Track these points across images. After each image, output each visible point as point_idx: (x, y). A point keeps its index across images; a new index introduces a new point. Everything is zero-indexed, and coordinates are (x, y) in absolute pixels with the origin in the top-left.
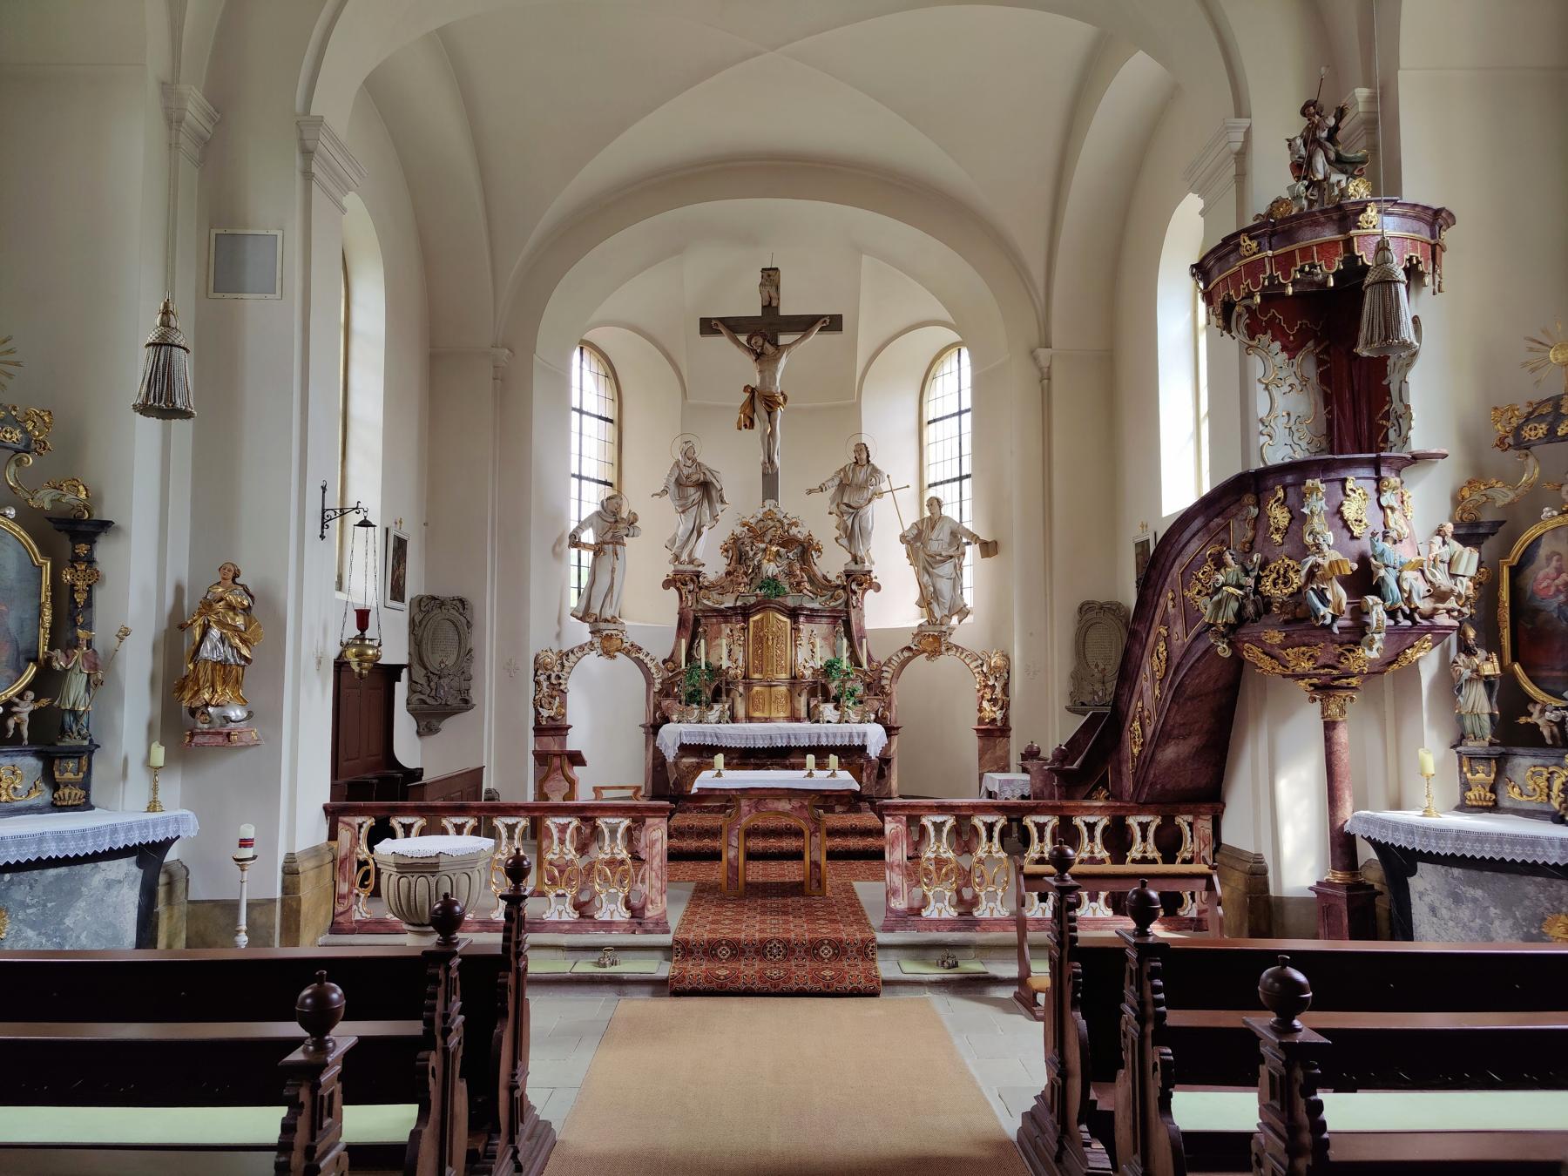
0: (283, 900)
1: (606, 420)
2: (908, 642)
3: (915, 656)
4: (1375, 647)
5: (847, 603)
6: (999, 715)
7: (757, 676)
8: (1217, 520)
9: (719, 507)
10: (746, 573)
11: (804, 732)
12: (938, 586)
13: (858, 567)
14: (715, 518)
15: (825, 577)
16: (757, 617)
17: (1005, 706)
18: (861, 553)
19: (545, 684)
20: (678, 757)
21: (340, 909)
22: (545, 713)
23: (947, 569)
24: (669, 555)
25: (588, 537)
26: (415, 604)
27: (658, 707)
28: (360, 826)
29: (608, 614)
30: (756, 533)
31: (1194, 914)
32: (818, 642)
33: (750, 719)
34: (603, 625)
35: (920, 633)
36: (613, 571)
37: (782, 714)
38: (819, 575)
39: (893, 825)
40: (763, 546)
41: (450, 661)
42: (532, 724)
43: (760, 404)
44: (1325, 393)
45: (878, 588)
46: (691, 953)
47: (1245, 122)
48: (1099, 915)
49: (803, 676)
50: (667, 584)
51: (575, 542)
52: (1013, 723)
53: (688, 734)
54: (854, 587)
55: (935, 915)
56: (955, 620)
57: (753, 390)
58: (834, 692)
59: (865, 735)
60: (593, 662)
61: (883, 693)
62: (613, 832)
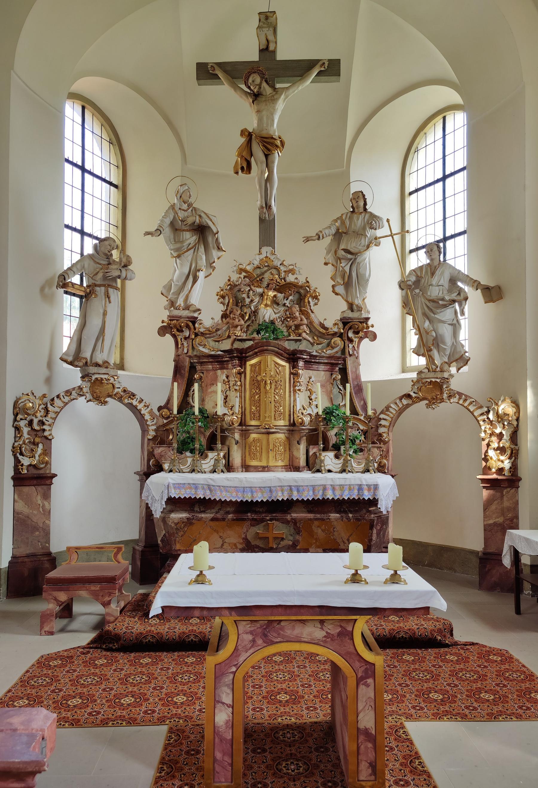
1: (111, 184)
2: (407, 389)
3: (414, 402)
5: (343, 351)
6: (507, 464)
7: (253, 423)
9: (215, 253)
10: (242, 316)
11: (305, 483)
12: (440, 331)
13: (355, 315)
14: (210, 265)
15: (322, 326)
16: (253, 361)
17: (514, 455)
18: (358, 301)
20: (166, 512)
22: (26, 461)
24: (164, 302)
27: (151, 455)
29: (99, 358)
30: (253, 278)
33: (246, 468)
34: (92, 369)
35: (420, 382)
36: (105, 314)
37: (280, 463)
40: (260, 290)
42: (9, 472)
45: (374, 337)
49: (302, 423)
50: (163, 331)
51: (63, 283)
52: (524, 472)
53: (178, 486)
54: (351, 334)
56: (453, 370)
58: (333, 440)
59: (376, 487)
61: (380, 441)
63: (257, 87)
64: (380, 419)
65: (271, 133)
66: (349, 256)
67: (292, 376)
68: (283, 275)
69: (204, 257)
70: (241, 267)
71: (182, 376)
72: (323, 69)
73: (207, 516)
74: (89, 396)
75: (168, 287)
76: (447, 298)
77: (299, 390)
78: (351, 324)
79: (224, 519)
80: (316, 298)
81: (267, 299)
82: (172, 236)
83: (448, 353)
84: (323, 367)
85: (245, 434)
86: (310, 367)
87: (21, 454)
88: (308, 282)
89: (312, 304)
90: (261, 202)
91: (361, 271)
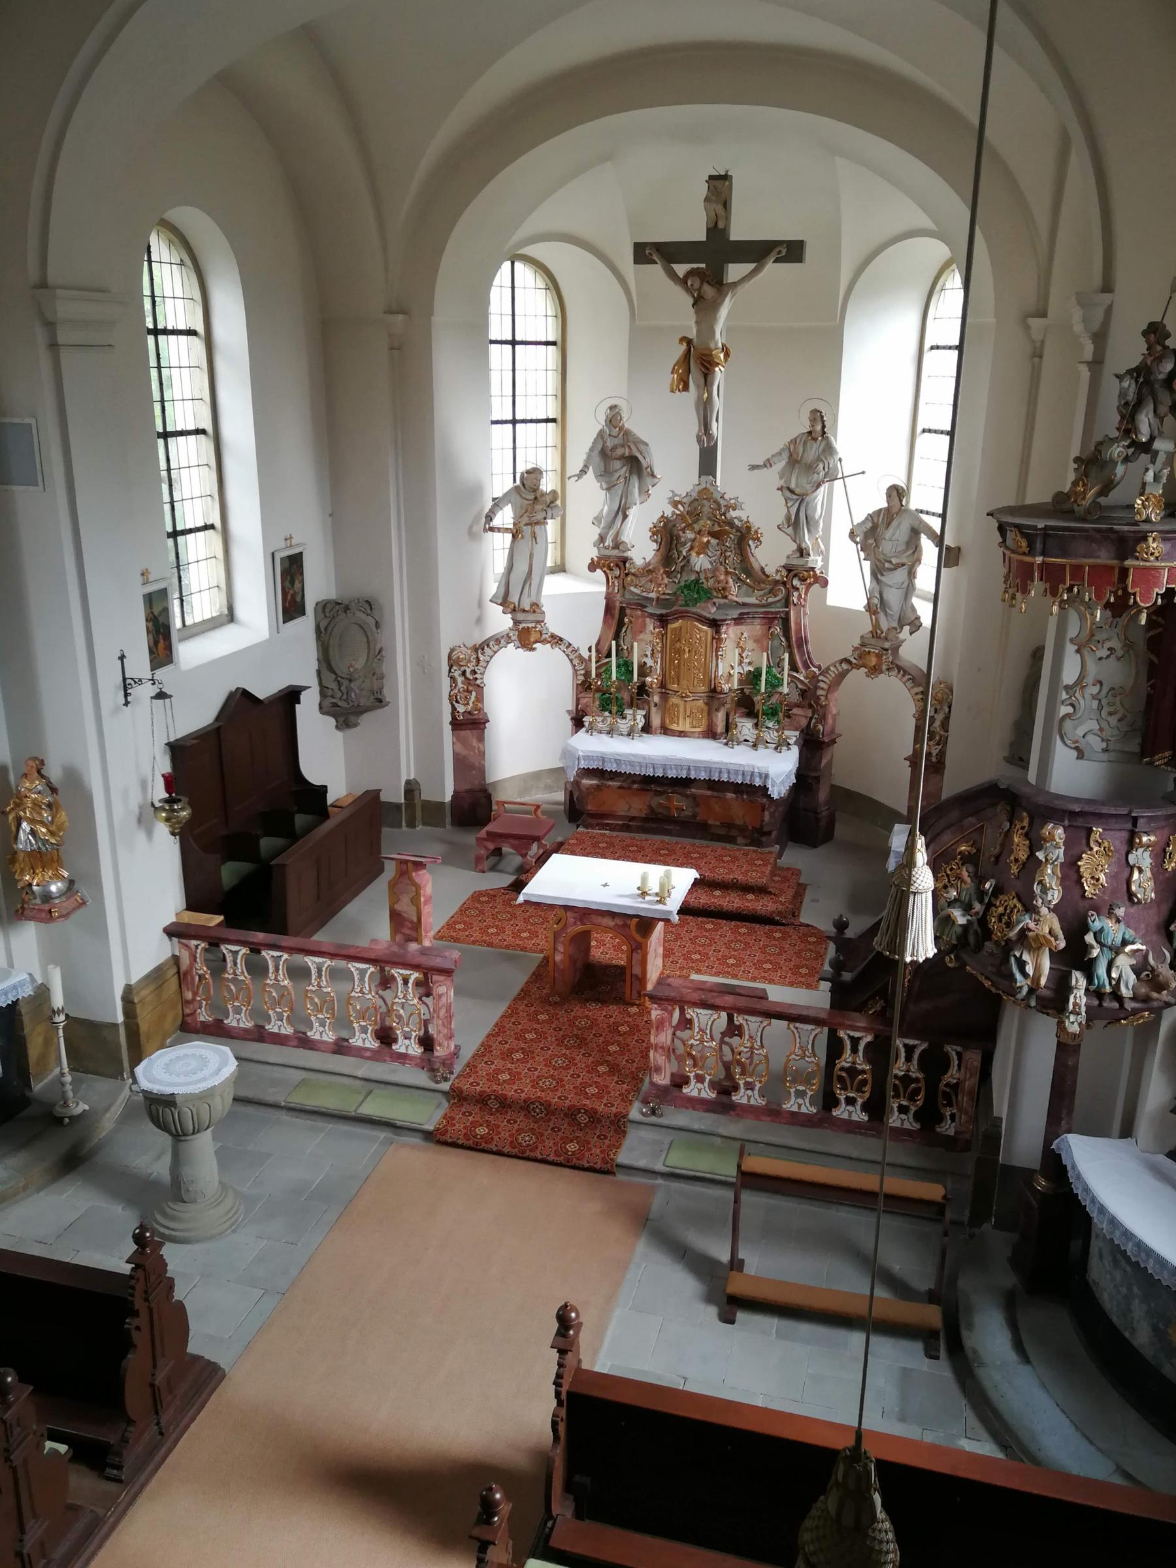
0: (126, 1024)
2: (848, 653)
8: (970, 819)
15: (762, 569)
19: (460, 679)
21: (187, 1011)
22: (461, 708)
23: (900, 575)
24: (596, 532)
25: (505, 517)
26: (320, 609)
28: (197, 947)
31: (951, 1132)
32: (750, 645)
33: (666, 731)
38: (756, 567)
39: (659, 1012)
41: (360, 664)
42: (447, 718)
43: (697, 363)
44: (1151, 663)
46: (465, 1099)
47: (1107, 298)
48: (855, 1117)
50: (592, 567)
54: (796, 582)
55: (695, 1093)
57: (689, 342)
60: (510, 654)
62: (406, 982)
64: (819, 681)
65: (712, 346)
69: (637, 485)
70: (677, 498)
71: (613, 616)
73: (615, 784)
74: (518, 643)
75: (597, 520)
76: (894, 561)
79: (629, 788)
82: (602, 465)
83: (897, 617)
85: (665, 696)
87: (457, 702)
91: (809, 512)
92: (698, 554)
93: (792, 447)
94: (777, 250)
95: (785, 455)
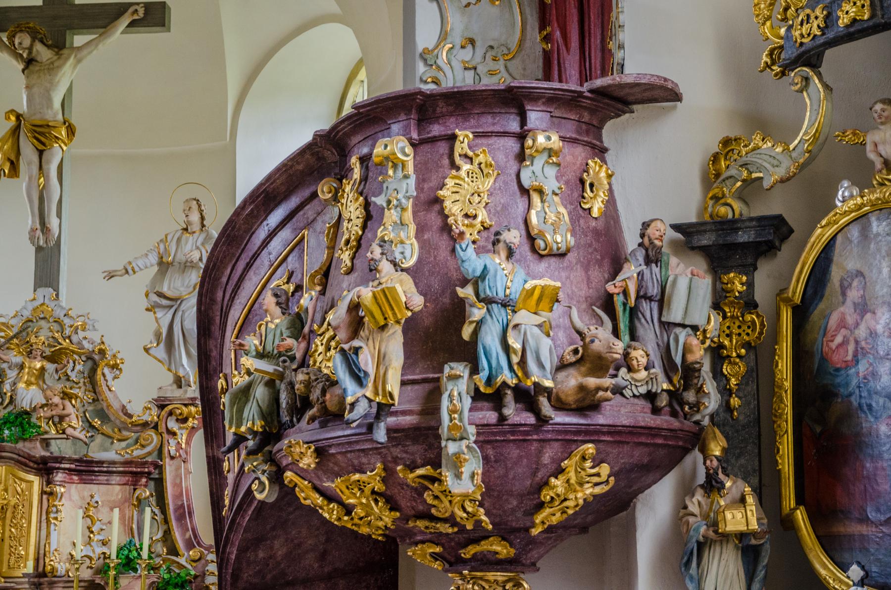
4: (466, 470)
38: (116, 405)
54: (172, 425)
57: (18, 117)
63: (27, 51)
66: (165, 302)
67: (45, 497)
68: (68, 332)
72: (137, 17)
77: (56, 519)
78: (170, 407)
80: (115, 367)
81: (28, 373)
84: (118, 478)
86: (92, 480)
88: (103, 343)
89: (109, 376)
90: (33, 222)
92: (29, 384)
93: (162, 246)
94: (131, 10)
95: (153, 259)
